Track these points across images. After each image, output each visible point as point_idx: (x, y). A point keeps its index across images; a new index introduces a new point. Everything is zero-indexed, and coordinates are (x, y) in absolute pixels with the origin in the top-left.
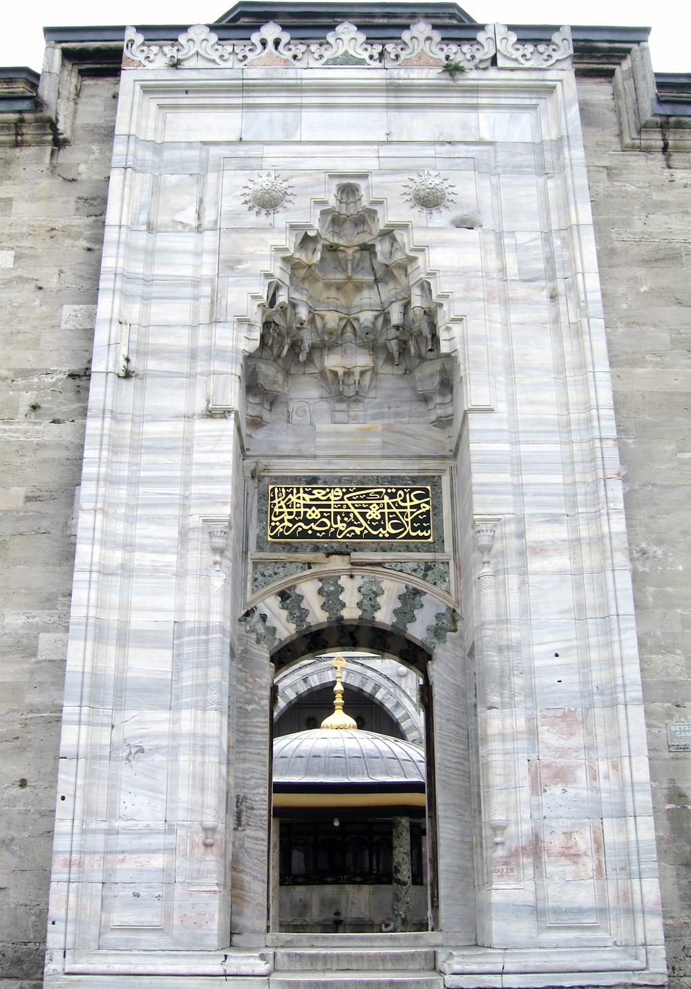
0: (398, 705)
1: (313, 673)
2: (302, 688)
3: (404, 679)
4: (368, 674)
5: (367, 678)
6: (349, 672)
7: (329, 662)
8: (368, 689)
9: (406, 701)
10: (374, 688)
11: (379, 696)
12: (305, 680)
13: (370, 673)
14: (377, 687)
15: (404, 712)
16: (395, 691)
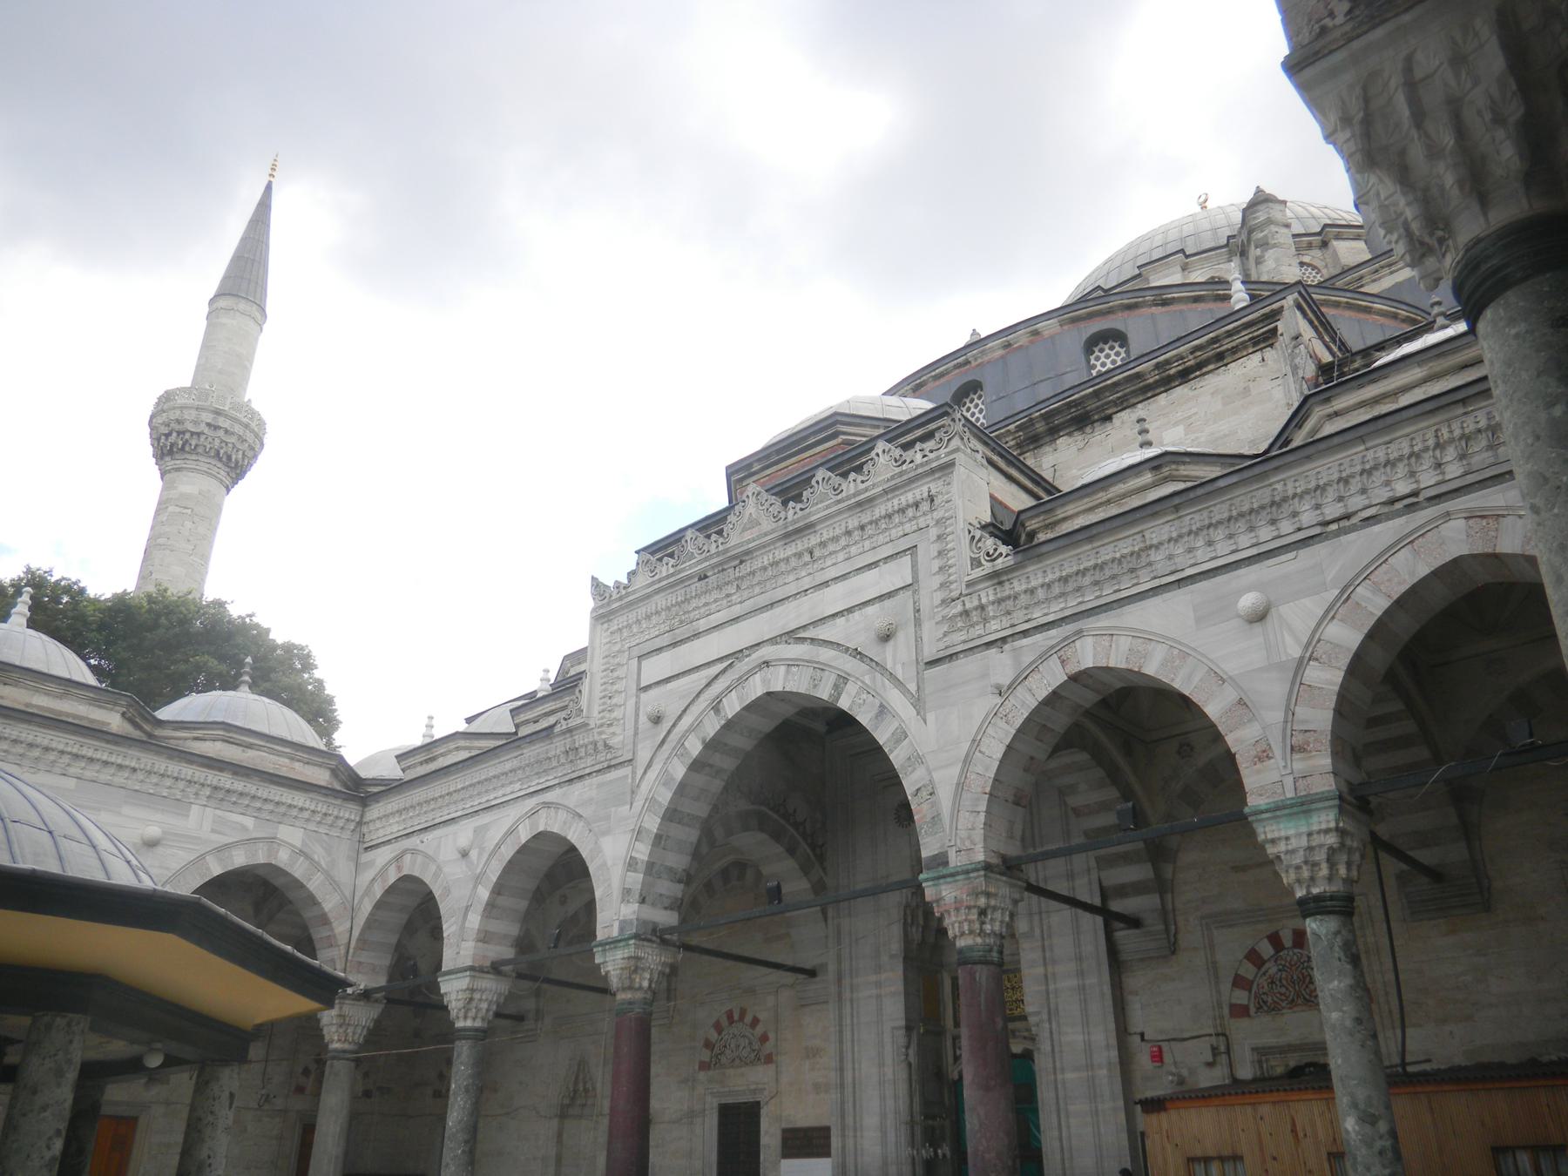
0: (883, 710)
1: (729, 690)
2: (712, 726)
3: (891, 643)
4: (821, 659)
5: (821, 667)
6: (791, 664)
7: (754, 656)
8: (824, 693)
9: (895, 699)
10: (836, 686)
11: (844, 704)
12: (716, 707)
13: (826, 654)
14: (843, 680)
15: (896, 724)
16: (874, 679)
